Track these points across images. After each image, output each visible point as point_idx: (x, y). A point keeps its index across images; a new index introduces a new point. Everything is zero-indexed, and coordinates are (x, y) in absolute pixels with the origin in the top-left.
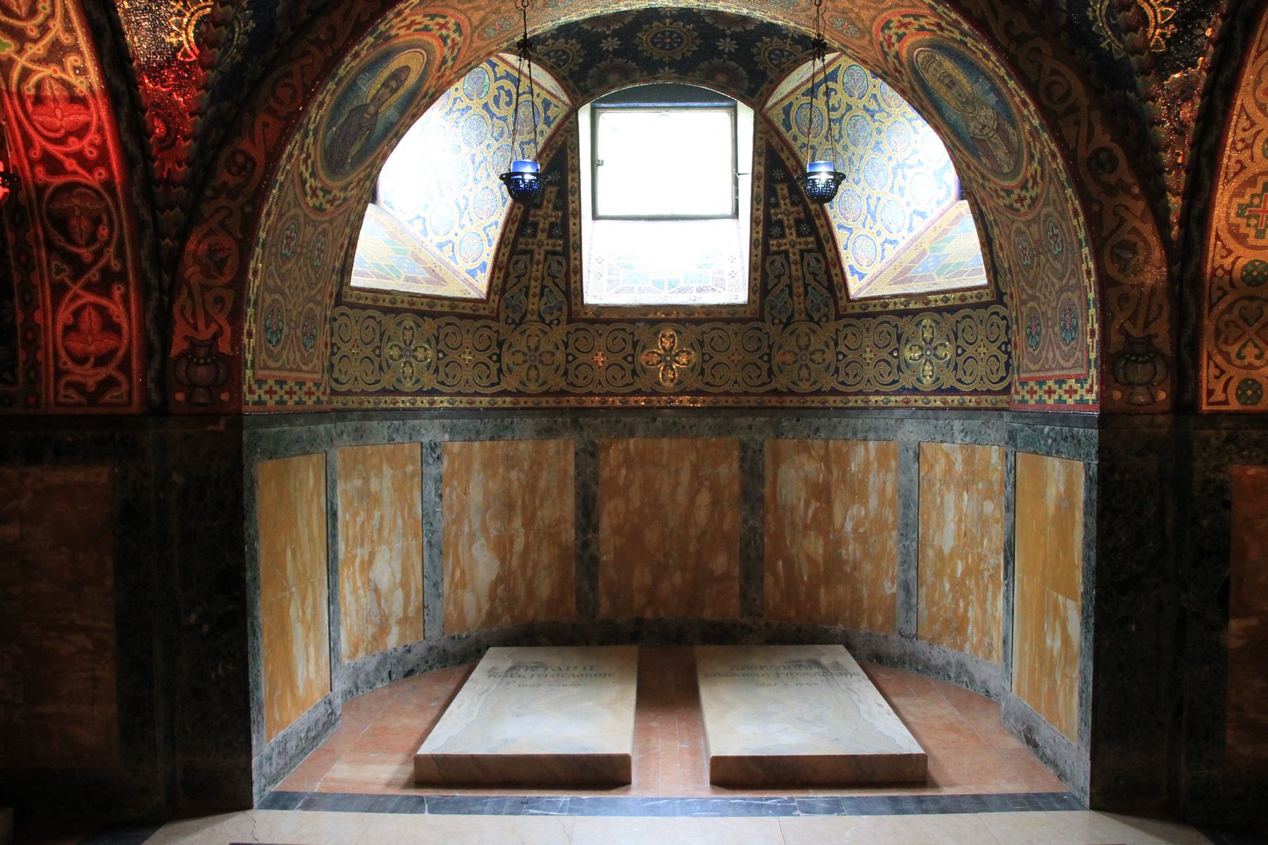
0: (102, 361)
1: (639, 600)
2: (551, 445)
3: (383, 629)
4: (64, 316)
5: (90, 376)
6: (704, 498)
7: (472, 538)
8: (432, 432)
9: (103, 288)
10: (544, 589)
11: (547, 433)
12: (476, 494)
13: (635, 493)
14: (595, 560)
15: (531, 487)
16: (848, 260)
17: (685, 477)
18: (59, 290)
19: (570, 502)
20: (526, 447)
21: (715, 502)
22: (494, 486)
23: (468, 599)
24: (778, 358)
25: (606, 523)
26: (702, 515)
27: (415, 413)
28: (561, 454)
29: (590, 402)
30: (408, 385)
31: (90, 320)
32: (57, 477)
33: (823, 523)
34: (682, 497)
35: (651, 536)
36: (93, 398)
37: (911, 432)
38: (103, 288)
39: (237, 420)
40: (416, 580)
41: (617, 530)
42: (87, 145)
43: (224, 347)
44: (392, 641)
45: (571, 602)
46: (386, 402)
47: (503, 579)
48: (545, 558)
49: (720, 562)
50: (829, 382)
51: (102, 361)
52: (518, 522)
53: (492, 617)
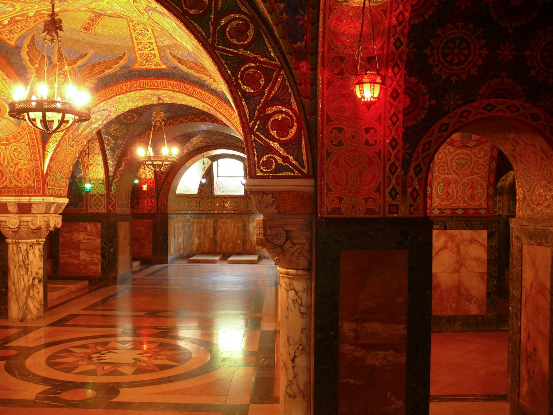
0: (151, 207)
1: (224, 248)
2: (208, 220)
3: (180, 250)
4: (146, 201)
5: (149, 208)
6: (236, 230)
7: (194, 236)
8: (188, 217)
9: (151, 198)
10: (207, 245)
11: (208, 218)
12: (195, 228)
13: (224, 229)
14: (216, 241)
15: (205, 227)
17: (233, 226)
18: (146, 198)
19: (212, 230)
20: (204, 220)
21: (238, 230)
22: (198, 227)
23: (194, 246)
24: (249, 205)
25: (218, 235)
26: (236, 233)
27: (185, 214)
28: (210, 222)
29: (216, 212)
30: (184, 209)
31: (150, 201)
32: (145, 221)
34: (232, 229)
35: (227, 237)
36: (150, 211)
38: (151, 198)
39: (167, 214)
40: (185, 242)
41: (220, 236)
42: (151, 181)
43: (165, 205)
44: (181, 251)
45: (212, 248)
46: (181, 212)
47: (199, 244)
48: (207, 240)
49: (239, 242)
51: (151, 207)
52: (202, 234)
53: (197, 250)
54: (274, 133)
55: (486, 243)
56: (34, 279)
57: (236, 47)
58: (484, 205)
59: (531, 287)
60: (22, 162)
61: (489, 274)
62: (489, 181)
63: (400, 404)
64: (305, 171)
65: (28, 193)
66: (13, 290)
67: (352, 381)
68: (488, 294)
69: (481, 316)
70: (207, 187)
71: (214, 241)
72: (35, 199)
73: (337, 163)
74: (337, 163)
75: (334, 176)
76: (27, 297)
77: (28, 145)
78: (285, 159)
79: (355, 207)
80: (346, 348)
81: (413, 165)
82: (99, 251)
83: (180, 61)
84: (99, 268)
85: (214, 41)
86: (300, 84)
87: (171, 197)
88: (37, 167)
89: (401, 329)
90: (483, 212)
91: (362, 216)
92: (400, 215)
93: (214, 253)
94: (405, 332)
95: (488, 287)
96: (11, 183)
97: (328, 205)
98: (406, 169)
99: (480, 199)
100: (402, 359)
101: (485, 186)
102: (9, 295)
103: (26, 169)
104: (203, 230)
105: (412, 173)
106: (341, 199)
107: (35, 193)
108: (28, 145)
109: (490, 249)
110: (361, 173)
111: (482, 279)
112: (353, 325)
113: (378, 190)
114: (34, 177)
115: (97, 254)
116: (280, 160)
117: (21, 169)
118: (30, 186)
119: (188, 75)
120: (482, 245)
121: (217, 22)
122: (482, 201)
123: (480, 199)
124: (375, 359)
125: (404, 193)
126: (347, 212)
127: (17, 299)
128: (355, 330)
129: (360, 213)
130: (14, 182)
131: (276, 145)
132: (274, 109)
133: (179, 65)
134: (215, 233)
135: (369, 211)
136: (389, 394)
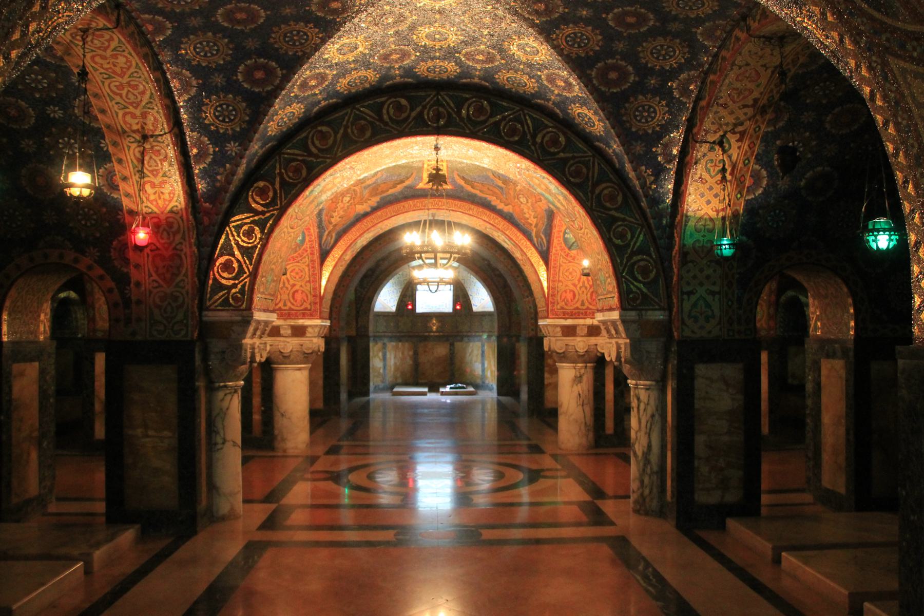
16: (473, 302)
65: (304, 316)
72: (307, 322)
77: (308, 266)
87: (371, 317)
88: (315, 289)
96: (285, 305)
103: (303, 291)
108: (308, 266)
117: (297, 291)
118: (306, 309)
130: (289, 304)
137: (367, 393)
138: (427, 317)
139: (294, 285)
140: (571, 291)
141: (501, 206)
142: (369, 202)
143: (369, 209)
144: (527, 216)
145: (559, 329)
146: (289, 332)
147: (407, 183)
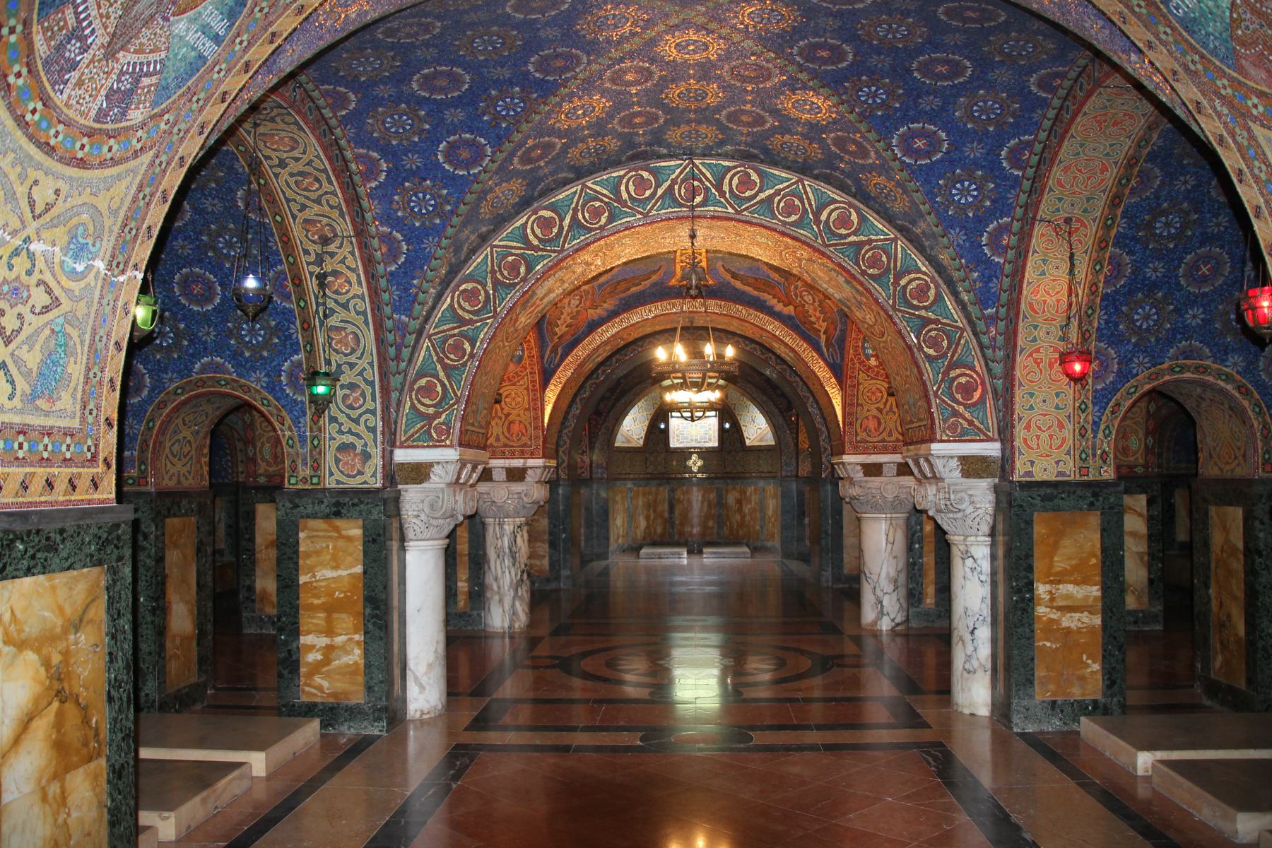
11: (660, 485)
12: (640, 502)
15: (655, 500)
16: (746, 435)
19: (666, 506)
20: (654, 489)
21: (709, 505)
25: (677, 512)
33: (740, 510)
37: (761, 483)
49: (711, 523)
50: (740, 469)
53: (644, 538)
54: (959, 397)
55: (1145, 512)
56: (523, 572)
57: (918, 308)
58: (1141, 461)
59: (1222, 551)
60: (515, 412)
61: (1151, 555)
62: (1147, 429)
63: (1096, 667)
64: (990, 434)
66: (495, 587)
67: (1048, 644)
68: (1151, 581)
69: (1142, 611)
70: (657, 431)
71: (670, 522)
73: (1028, 427)
74: (1028, 427)
75: (1025, 440)
76: (514, 598)
77: (527, 389)
78: (971, 423)
79: (1045, 471)
80: (1041, 610)
81: (1102, 427)
82: (546, 537)
83: (734, 276)
84: (546, 562)
85: (894, 302)
86: (988, 348)
88: (535, 419)
89: (1095, 591)
90: (1139, 470)
91: (1054, 479)
92: (1091, 478)
93: (678, 544)
94: (1099, 594)
95: (1150, 573)
96: (498, 439)
97: (1020, 470)
98: (1095, 432)
99: (1136, 453)
100: (1097, 621)
101: (1141, 435)
102: (488, 594)
104: (651, 506)
105: (1100, 435)
106: (1032, 463)
107: (532, 453)
108: (527, 389)
109: (1150, 520)
110: (1051, 436)
111: (1142, 560)
112: (1048, 587)
113: (1068, 453)
114: (531, 430)
115: (543, 542)
116: (965, 424)
119: (744, 293)
120: (1140, 515)
121: (896, 282)
122: (1138, 455)
123: (1136, 453)
124: (1069, 621)
125: (1094, 455)
126: (1039, 476)
127: (501, 601)
128: (1050, 592)
129: (1050, 476)
130: (503, 439)
131: (961, 409)
132: (958, 371)
133: (733, 281)
134: (671, 509)
135: (1060, 473)
136: (1085, 657)
137: (604, 556)
138: (685, 453)
139: (508, 415)
140: (875, 417)
141: (779, 307)
142: (605, 305)
143: (605, 314)
144: (813, 319)
145: (859, 468)
146: (504, 477)
147: (654, 278)
